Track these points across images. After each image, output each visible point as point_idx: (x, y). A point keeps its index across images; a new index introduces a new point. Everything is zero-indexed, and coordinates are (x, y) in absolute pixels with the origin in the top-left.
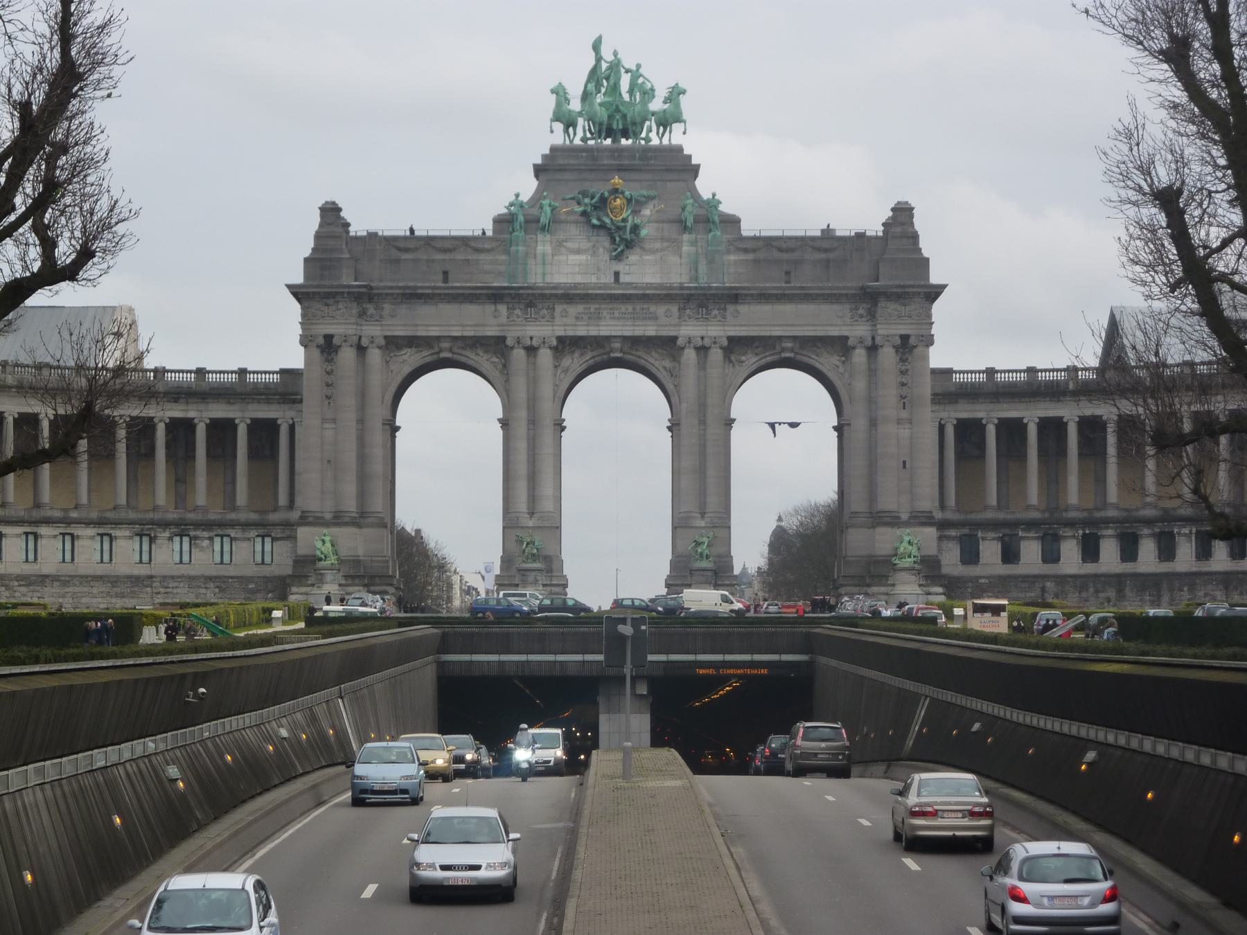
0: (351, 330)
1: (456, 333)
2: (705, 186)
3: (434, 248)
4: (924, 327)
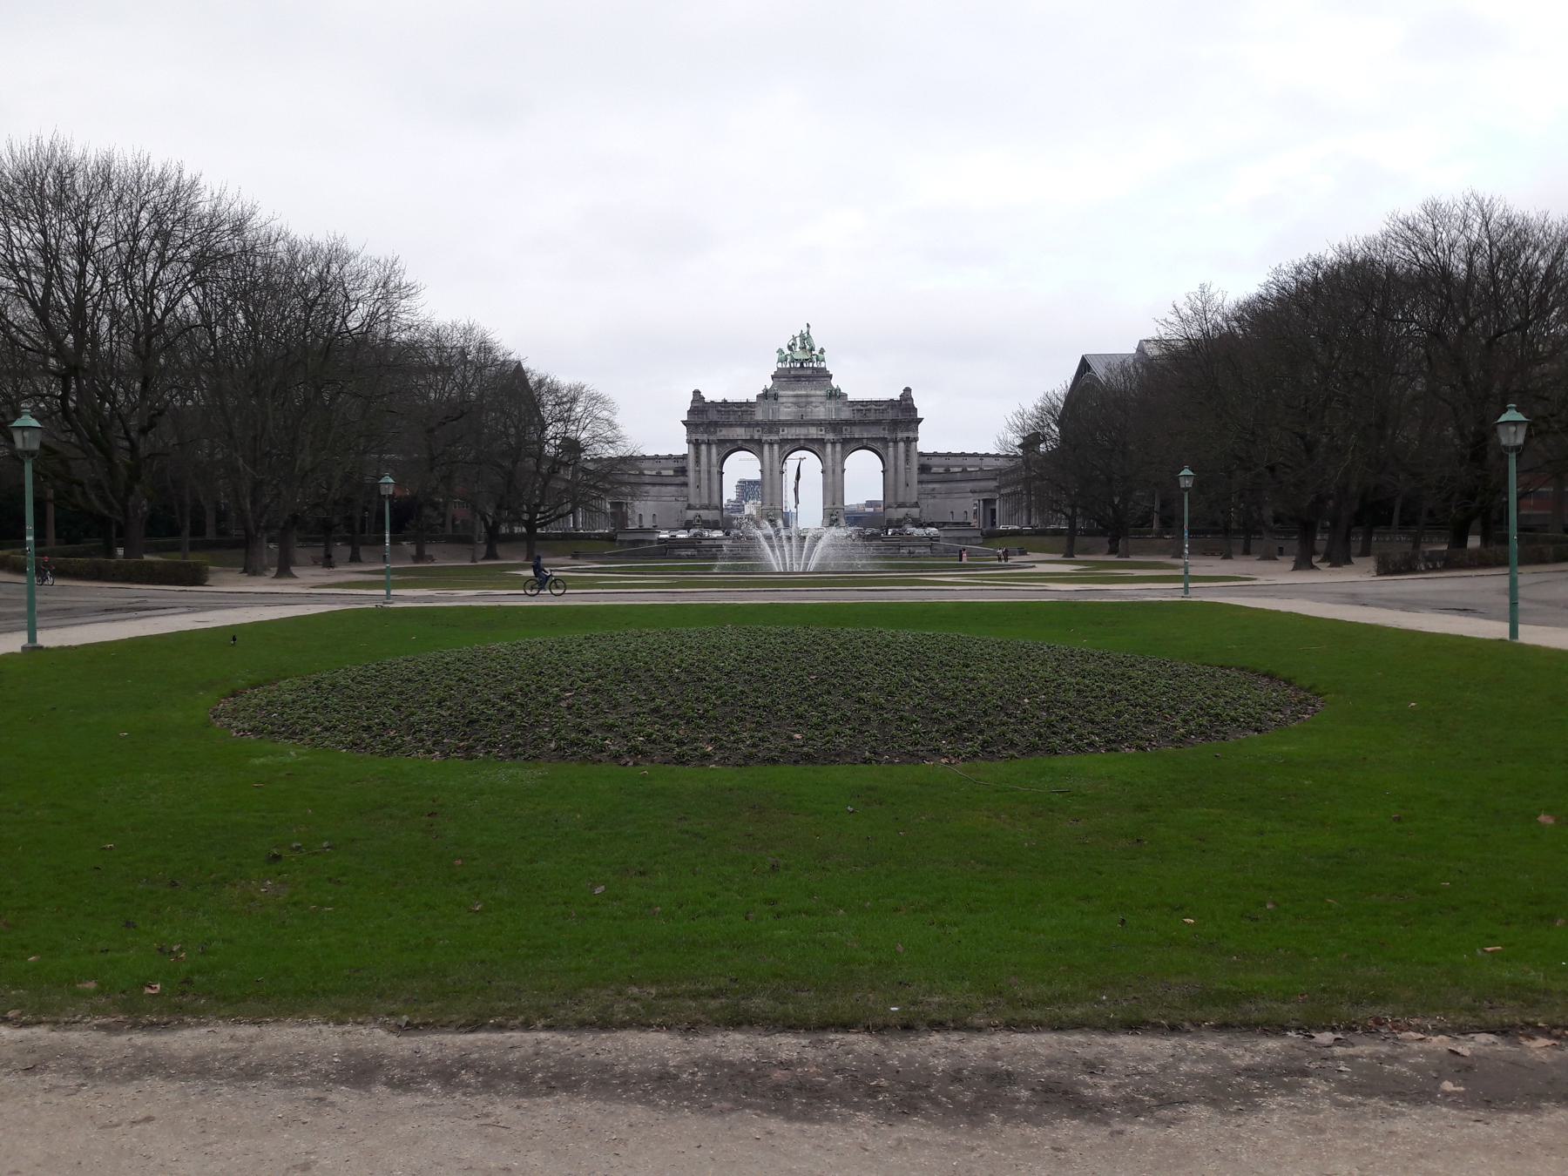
0: (705, 437)
2: (835, 383)
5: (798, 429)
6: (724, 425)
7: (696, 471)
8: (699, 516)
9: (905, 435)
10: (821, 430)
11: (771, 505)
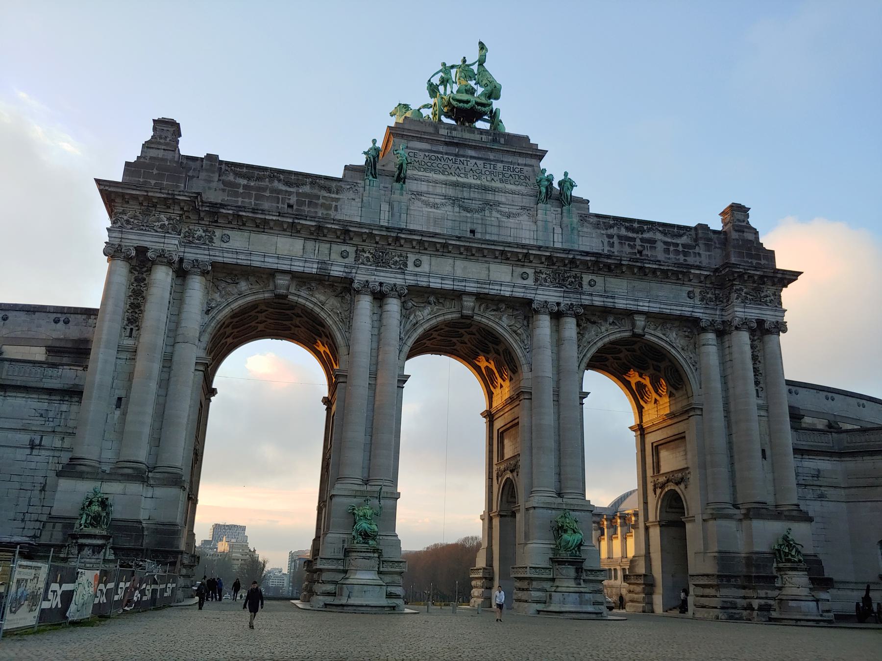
0: (172, 244)
1: (298, 267)
3: (279, 181)
4: (780, 314)
5: (459, 264)
6: (239, 222)
7: (120, 349)
8: (104, 504)
9: (753, 313)
10: (524, 276)
11: (366, 482)
